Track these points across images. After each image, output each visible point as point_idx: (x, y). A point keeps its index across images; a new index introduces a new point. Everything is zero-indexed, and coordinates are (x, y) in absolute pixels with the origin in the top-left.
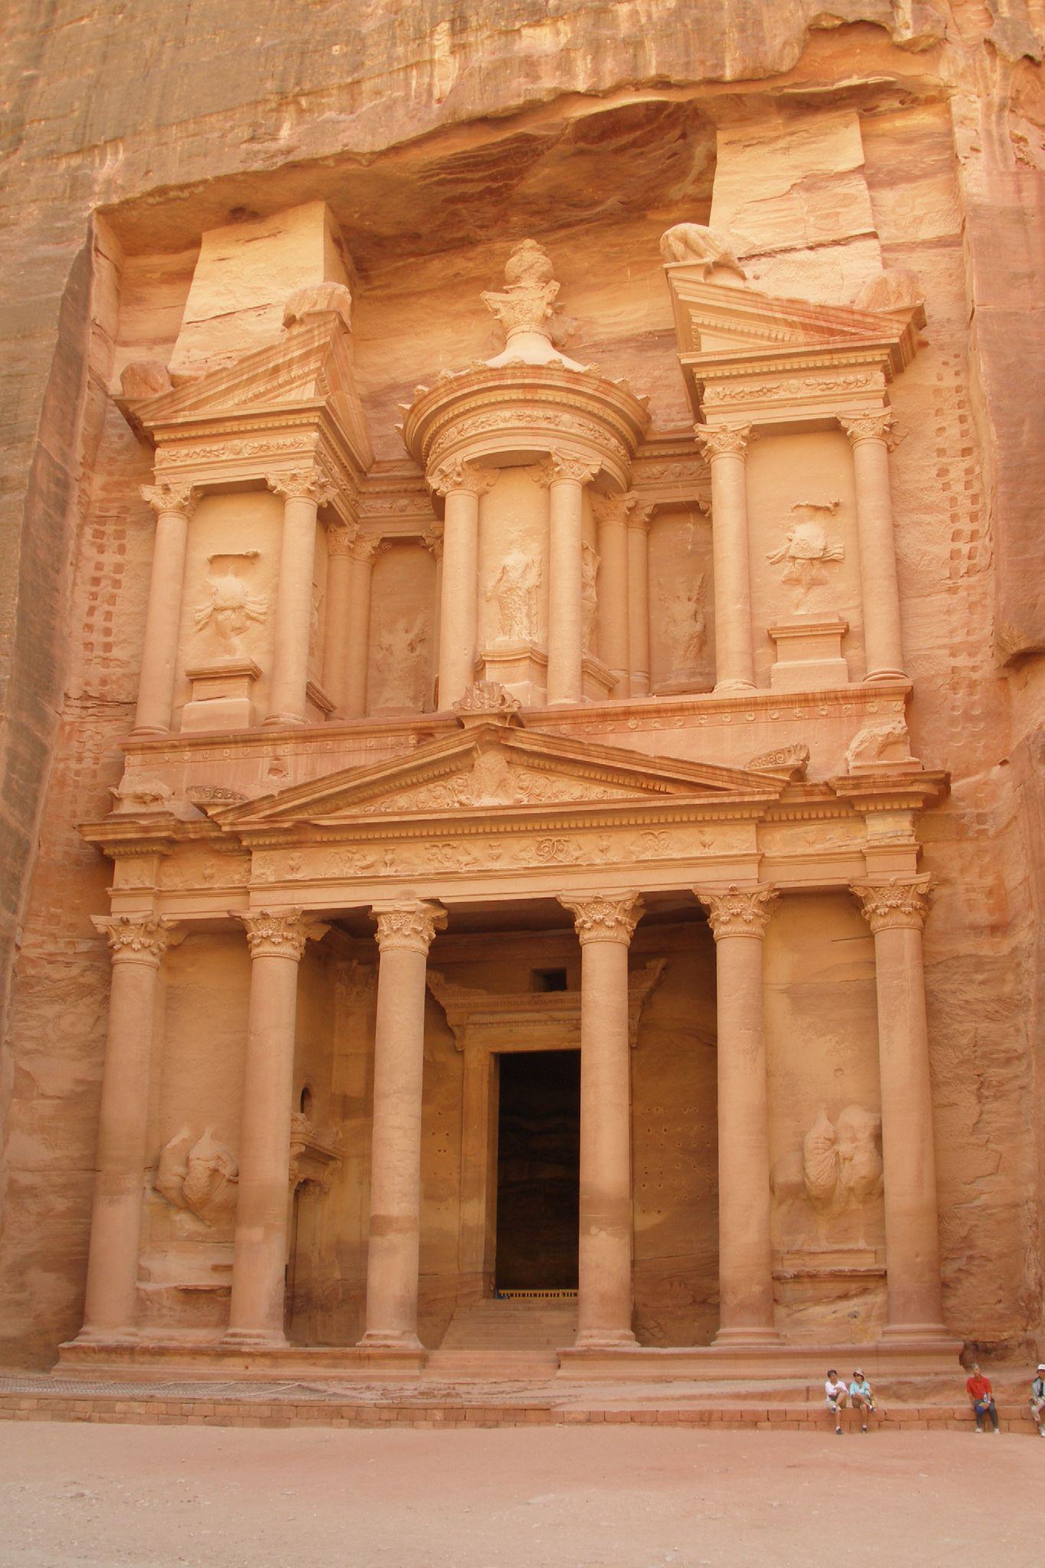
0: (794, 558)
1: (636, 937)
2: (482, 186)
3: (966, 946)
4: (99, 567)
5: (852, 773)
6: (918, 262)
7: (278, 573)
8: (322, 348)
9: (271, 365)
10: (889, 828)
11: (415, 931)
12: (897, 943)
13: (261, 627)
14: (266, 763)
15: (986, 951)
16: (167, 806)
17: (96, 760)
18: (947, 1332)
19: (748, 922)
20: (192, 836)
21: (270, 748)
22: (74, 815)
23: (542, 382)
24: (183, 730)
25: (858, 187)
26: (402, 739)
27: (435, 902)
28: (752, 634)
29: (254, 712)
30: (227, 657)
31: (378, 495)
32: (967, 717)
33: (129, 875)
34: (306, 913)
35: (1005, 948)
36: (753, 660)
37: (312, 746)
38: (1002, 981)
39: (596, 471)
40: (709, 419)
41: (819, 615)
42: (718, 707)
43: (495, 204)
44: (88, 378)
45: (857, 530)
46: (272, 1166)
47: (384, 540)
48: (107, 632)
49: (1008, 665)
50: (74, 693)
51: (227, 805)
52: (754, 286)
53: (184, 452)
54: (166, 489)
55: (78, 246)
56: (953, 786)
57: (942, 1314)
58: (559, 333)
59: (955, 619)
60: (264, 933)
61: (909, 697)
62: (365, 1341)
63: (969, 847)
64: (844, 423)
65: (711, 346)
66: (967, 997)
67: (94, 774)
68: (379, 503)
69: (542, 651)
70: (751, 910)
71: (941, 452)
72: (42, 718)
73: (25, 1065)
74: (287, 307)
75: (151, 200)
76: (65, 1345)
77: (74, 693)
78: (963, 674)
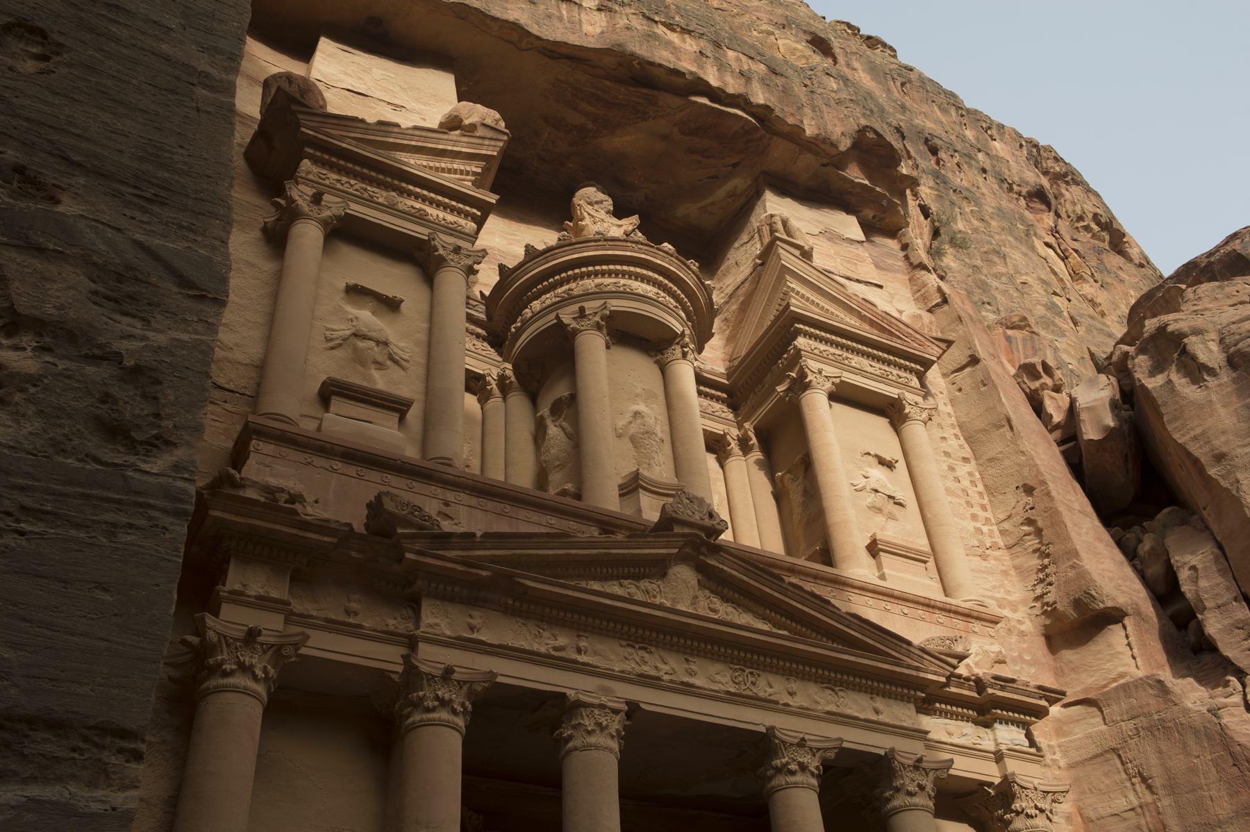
0: (876, 491)
9: (441, 147)
10: (1008, 735)
13: (402, 373)
16: (309, 510)
20: (354, 554)
21: (439, 490)
25: (863, 252)
26: (584, 528)
27: (633, 709)
42: (864, 589)
51: (421, 528)
53: (335, 177)
54: (317, 199)
60: (447, 696)
70: (929, 786)
71: (947, 454)
78: (1013, 623)
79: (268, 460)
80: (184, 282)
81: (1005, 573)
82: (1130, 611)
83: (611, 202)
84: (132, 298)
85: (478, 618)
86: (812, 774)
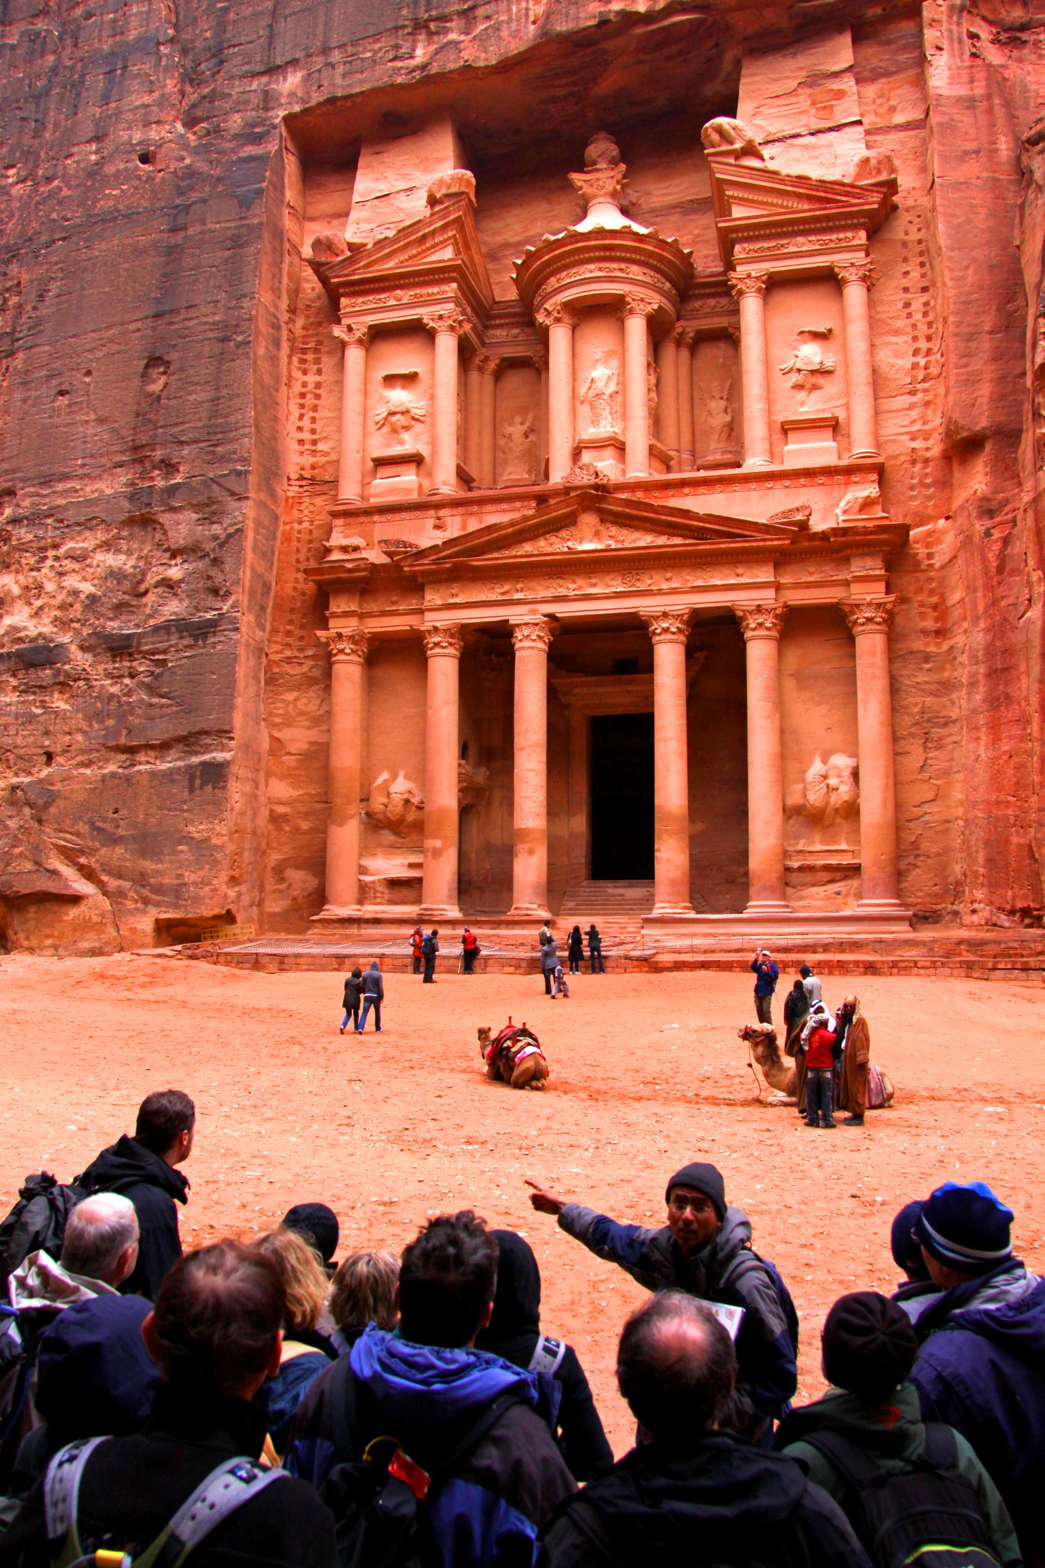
0: (799, 371)
1: (688, 638)
2: (567, 90)
3: (918, 644)
4: (305, 385)
5: (842, 525)
6: (890, 143)
7: (433, 386)
8: (458, 220)
11: (539, 637)
12: (870, 646)
13: (422, 426)
14: (431, 522)
15: (932, 649)
16: (364, 554)
17: (312, 522)
18: (900, 905)
19: (768, 629)
22: (298, 561)
23: (617, 242)
24: (372, 500)
27: (551, 617)
28: (770, 424)
29: (420, 486)
30: (399, 448)
31: (497, 327)
32: (922, 484)
33: (339, 605)
34: (464, 627)
35: (945, 647)
36: (771, 444)
37: (461, 510)
38: (942, 668)
39: (656, 307)
40: (739, 268)
41: (817, 412)
43: (576, 104)
44: (287, 246)
45: (845, 349)
46: (446, 797)
47: (504, 360)
48: (313, 431)
49: (953, 447)
50: (294, 476)
52: (771, 165)
53: (361, 300)
54: (350, 329)
55: (273, 147)
56: (911, 533)
57: (898, 893)
58: (625, 203)
59: (914, 414)
60: (435, 640)
61: (880, 472)
62: (513, 912)
63: (922, 576)
64: (836, 270)
65: (738, 212)
66: (918, 680)
67: (311, 532)
68: (499, 332)
69: (621, 438)
71: (906, 290)
72: (272, 493)
73: (276, 734)
74: (430, 190)
75: (324, 109)
76: (314, 918)
77: (294, 476)
79: (341, 529)
80: (233, 494)
81: (927, 404)
82: (988, 432)
83: (613, 147)
84: (214, 513)
85: (455, 588)
86: (673, 633)
